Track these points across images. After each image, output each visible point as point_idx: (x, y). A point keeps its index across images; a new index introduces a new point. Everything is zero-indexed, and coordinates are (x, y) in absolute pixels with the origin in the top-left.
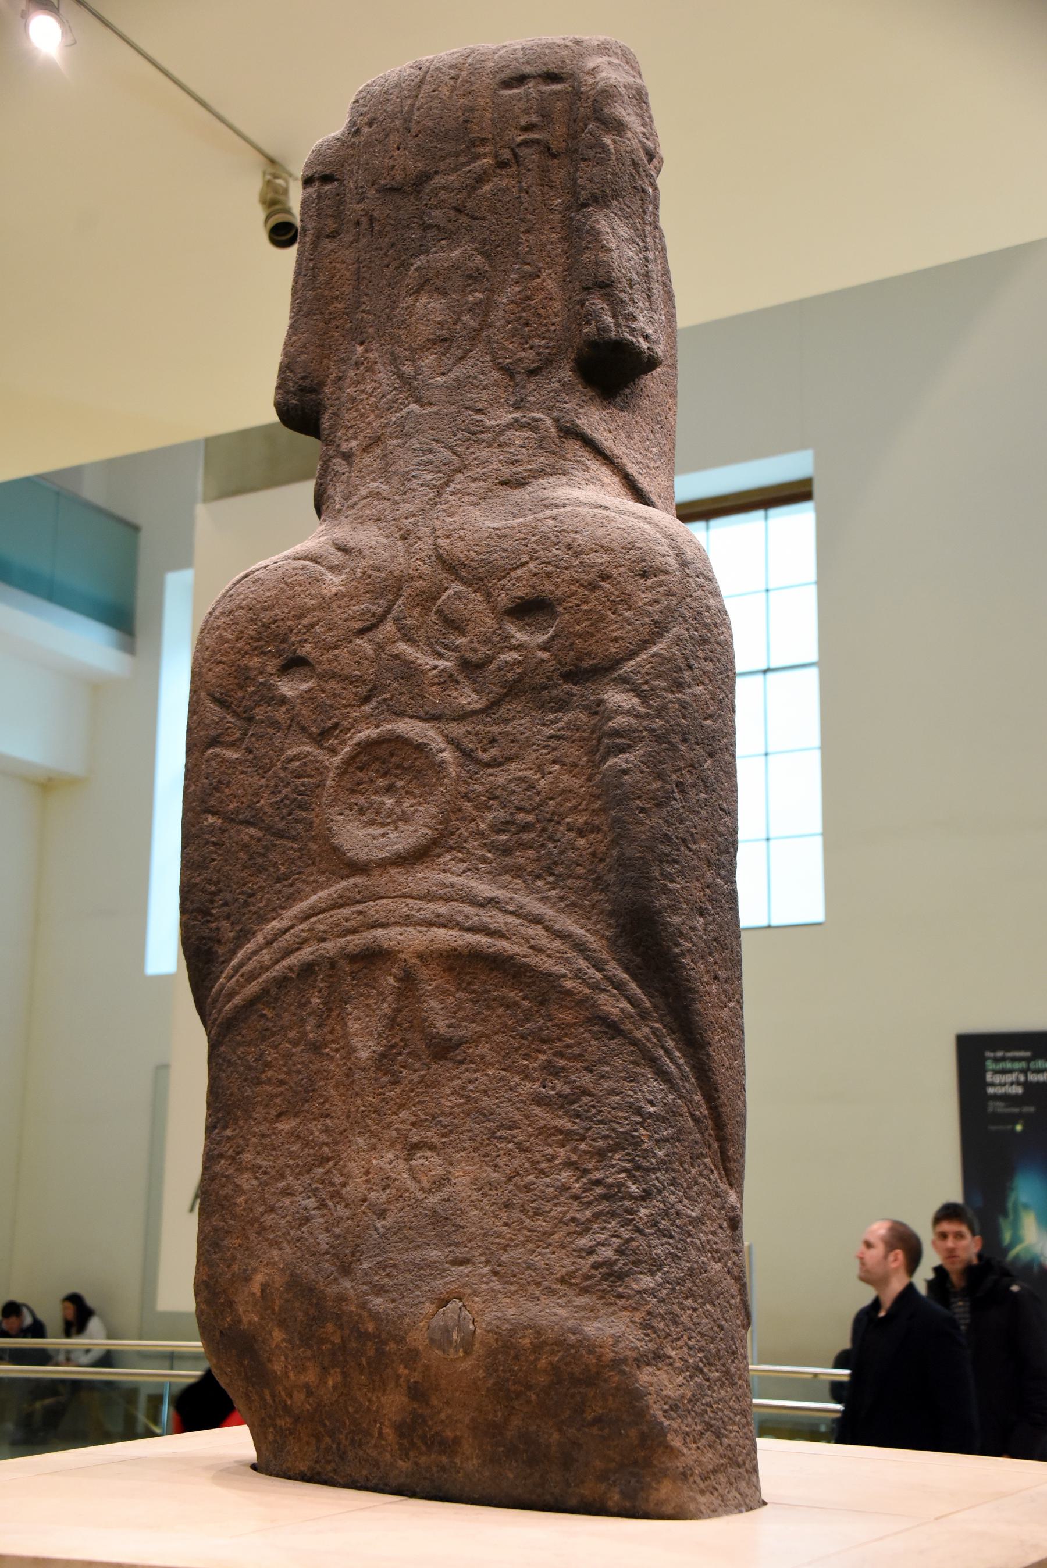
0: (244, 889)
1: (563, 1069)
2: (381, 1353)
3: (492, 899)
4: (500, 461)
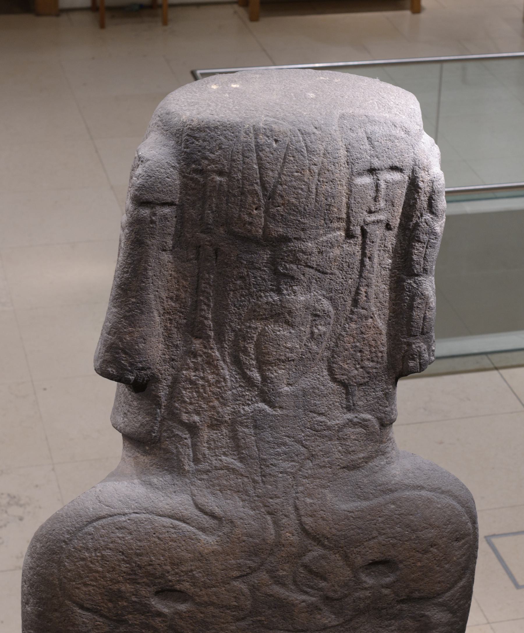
4: (339, 452)
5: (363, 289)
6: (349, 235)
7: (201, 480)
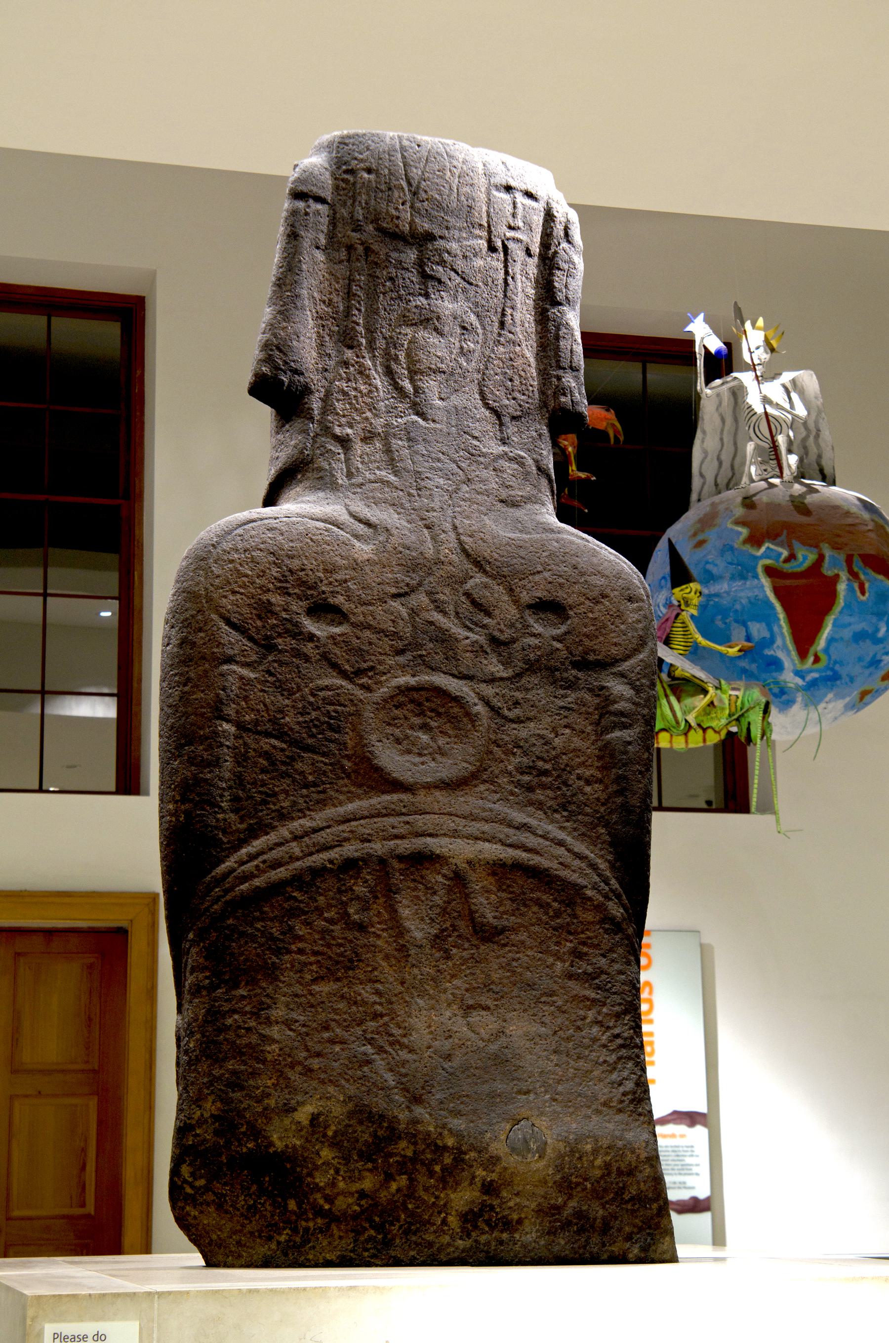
0: (261, 789)
1: (586, 954)
2: (459, 1160)
3: (525, 824)
5: (509, 311)
6: (492, 249)
7: (354, 493)
